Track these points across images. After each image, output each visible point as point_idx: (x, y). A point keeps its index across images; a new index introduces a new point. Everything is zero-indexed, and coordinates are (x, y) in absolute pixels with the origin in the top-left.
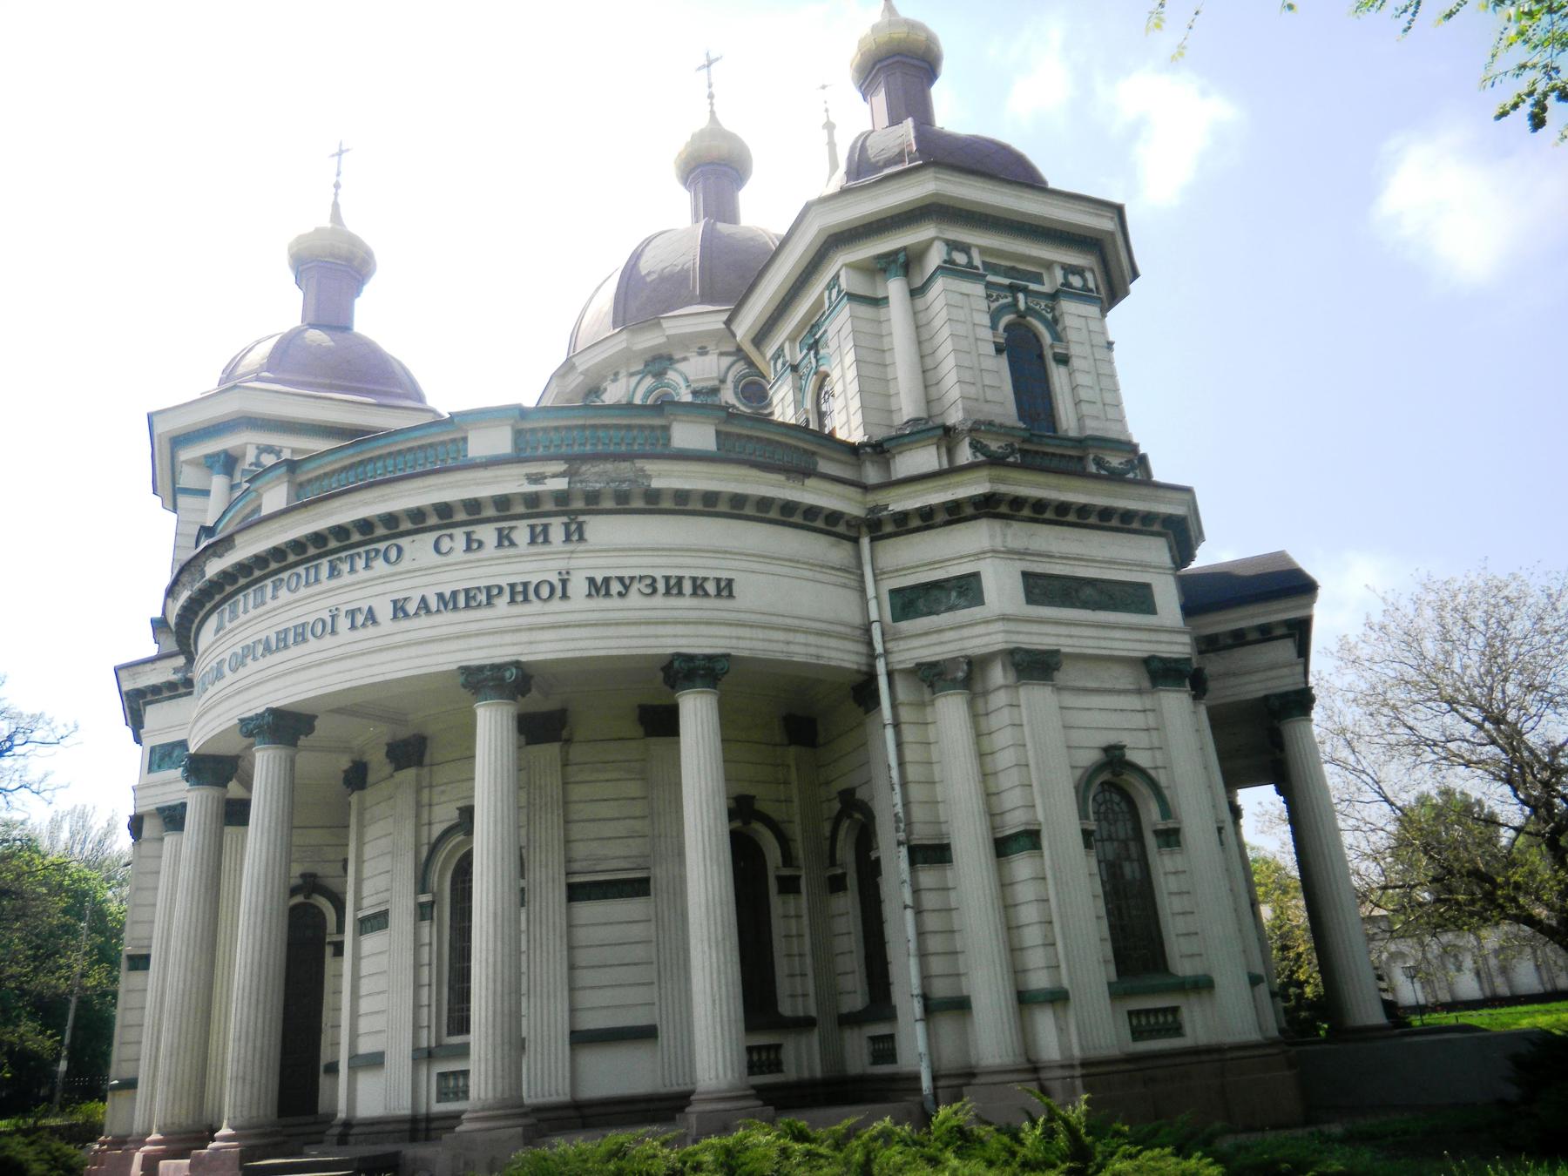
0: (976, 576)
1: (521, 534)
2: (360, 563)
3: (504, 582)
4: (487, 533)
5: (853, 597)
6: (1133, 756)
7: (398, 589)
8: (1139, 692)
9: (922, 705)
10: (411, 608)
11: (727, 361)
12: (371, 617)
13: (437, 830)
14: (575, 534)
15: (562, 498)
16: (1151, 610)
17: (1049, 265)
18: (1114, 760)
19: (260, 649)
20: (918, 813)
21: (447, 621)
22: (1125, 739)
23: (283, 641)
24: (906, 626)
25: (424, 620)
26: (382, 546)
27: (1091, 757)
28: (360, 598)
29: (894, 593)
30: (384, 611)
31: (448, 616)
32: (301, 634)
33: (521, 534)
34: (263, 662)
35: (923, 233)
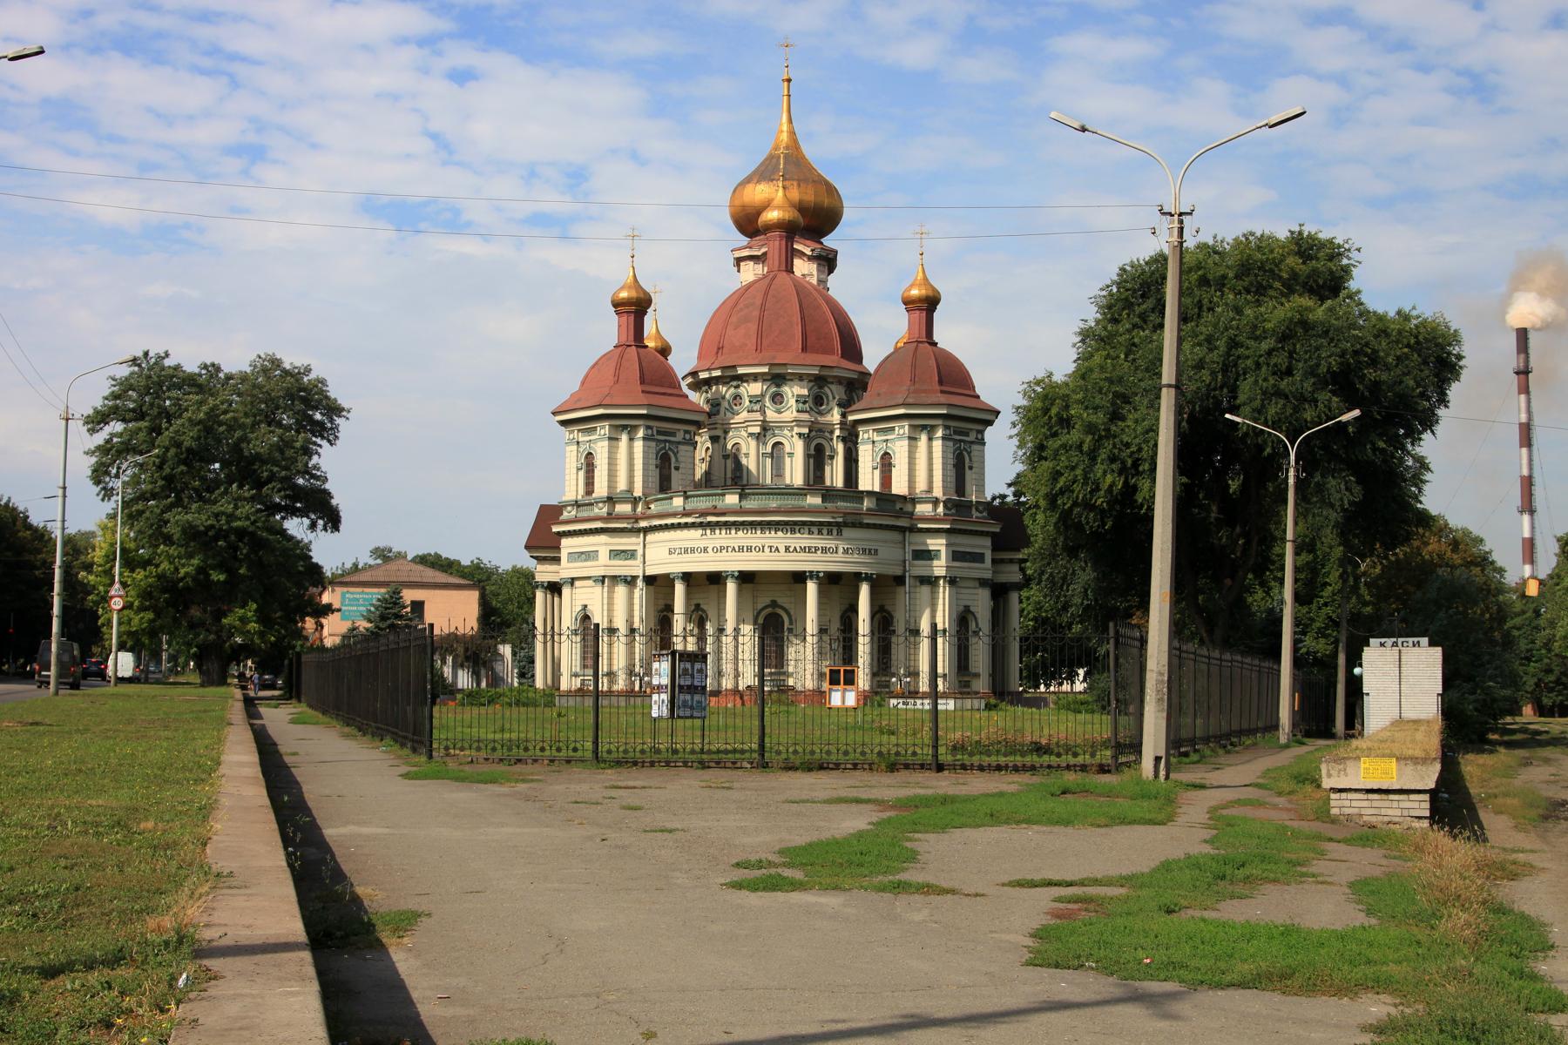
0: (939, 551)
1: (825, 531)
2: (773, 532)
3: (820, 546)
4: (815, 529)
5: (901, 551)
6: (972, 609)
7: (788, 542)
8: (975, 588)
9: (916, 587)
10: (791, 549)
11: (811, 384)
12: (777, 549)
13: (760, 606)
14: (840, 533)
15: (838, 524)
16: (983, 562)
17: (971, 430)
18: (967, 610)
19: (730, 549)
20: (912, 621)
21: (803, 556)
22: (968, 603)
23: (741, 549)
24: (916, 562)
25: (795, 554)
26: (781, 527)
27: (961, 608)
28: (774, 543)
29: (913, 551)
30: (782, 549)
31: (802, 554)
32: (749, 549)
33: (825, 531)
34: (730, 553)
35: (939, 422)
